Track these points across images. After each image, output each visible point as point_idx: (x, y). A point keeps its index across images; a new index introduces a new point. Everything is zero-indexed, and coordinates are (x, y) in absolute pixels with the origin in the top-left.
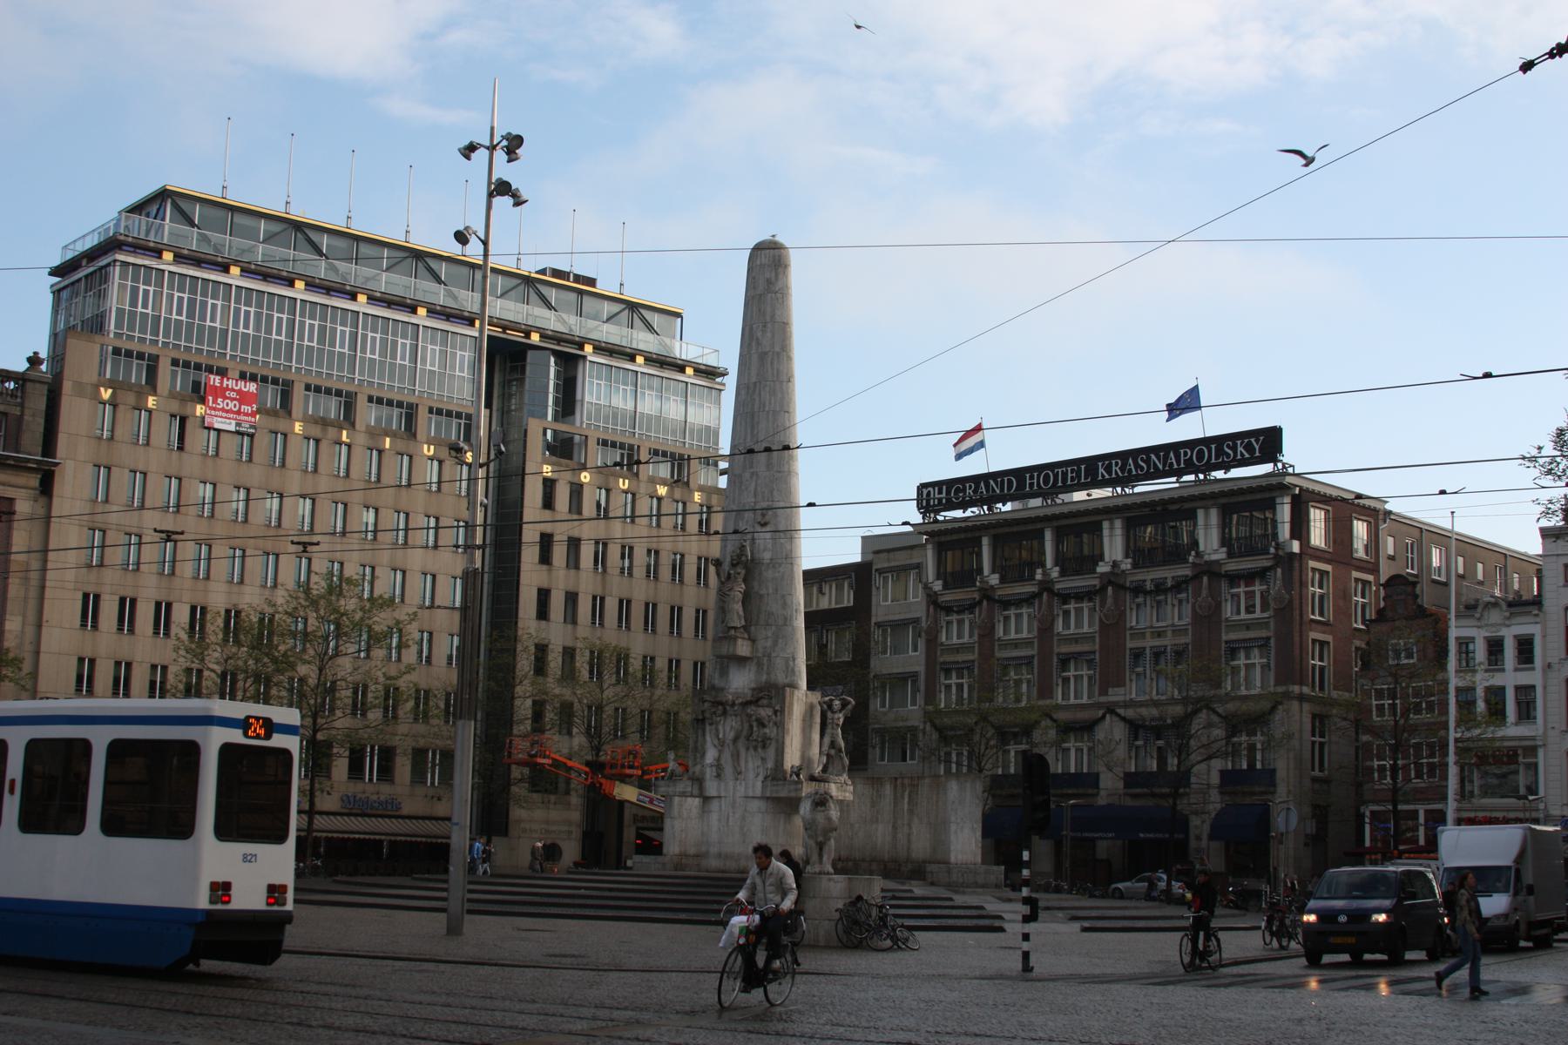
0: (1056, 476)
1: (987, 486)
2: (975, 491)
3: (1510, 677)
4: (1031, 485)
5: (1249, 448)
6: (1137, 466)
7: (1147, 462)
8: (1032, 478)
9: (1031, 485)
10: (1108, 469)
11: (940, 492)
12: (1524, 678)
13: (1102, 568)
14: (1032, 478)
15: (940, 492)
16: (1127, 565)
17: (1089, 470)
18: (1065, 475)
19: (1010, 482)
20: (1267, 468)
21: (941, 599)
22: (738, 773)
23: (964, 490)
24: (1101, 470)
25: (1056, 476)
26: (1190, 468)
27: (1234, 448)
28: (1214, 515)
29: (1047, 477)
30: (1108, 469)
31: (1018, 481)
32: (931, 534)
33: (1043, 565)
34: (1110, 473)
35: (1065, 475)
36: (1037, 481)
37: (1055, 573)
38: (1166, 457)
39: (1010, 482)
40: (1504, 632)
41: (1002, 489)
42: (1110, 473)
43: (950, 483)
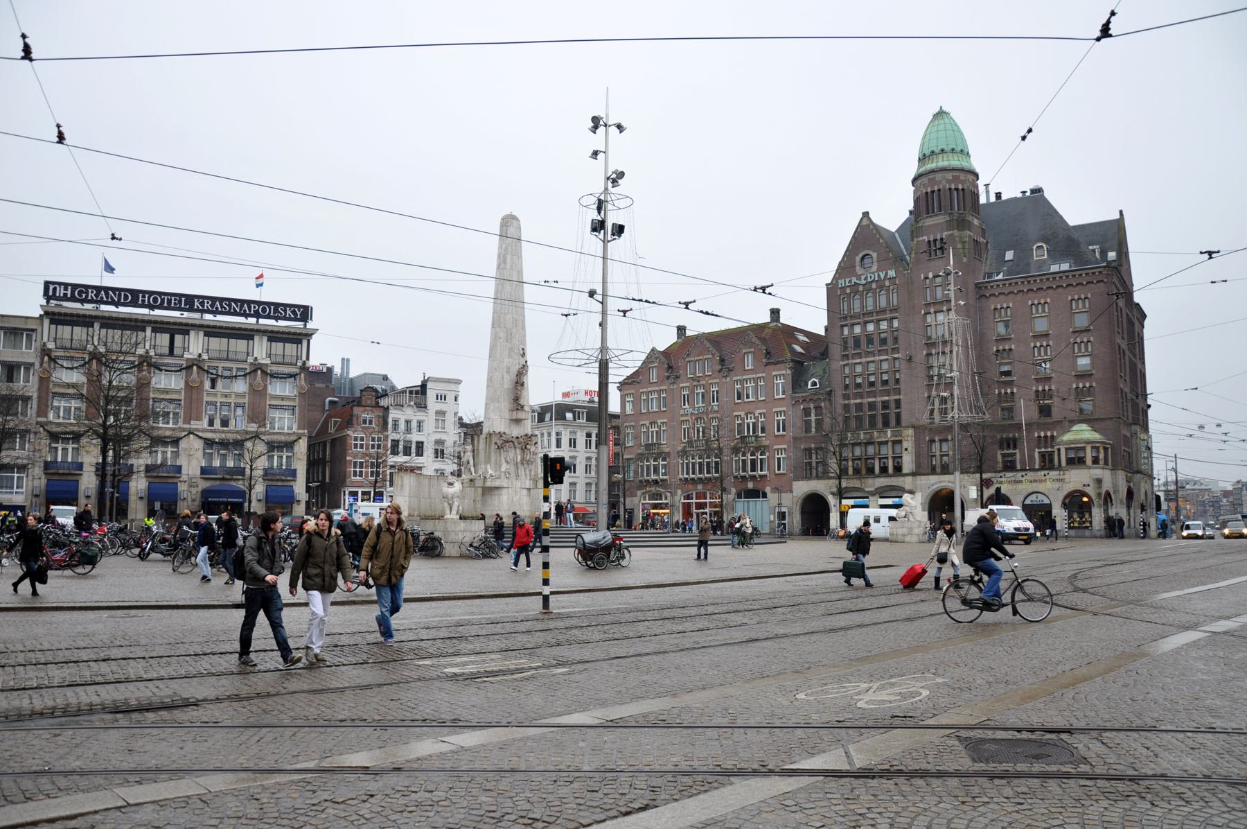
0: (163, 300)
2: (97, 296)
5: (294, 312)
7: (230, 306)
10: (202, 304)
11: (66, 289)
15: (66, 289)
17: (188, 301)
18: (169, 301)
20: (299, 324)
21: (53, 354)
22: (517, 475)
23: (87, 293)
25: (163, 300)
26: (257, 315)
27: (285, 311)
28: (265, 339)
30: (202, 304)
35: (169, 301)
43: (75, 286)
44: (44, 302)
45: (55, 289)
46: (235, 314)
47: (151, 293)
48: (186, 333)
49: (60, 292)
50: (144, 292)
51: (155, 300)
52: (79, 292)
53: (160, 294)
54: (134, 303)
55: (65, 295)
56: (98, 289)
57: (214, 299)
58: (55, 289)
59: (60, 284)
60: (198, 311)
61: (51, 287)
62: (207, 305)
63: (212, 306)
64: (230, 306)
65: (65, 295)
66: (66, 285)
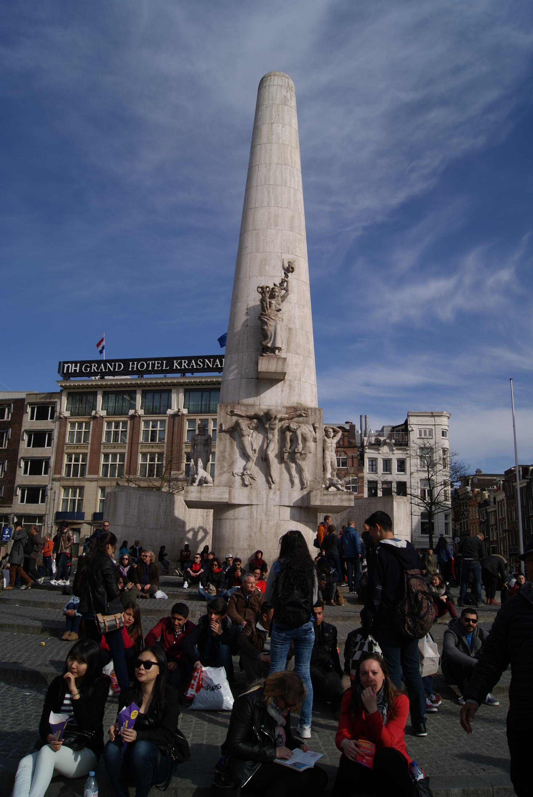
0: (148, 365)
1: (105, 366)
2: (97, 369)
3: (395, 476)
4: (133, 368)
6: (197, 364)
7: (204, 363)
8: (133, 364)
9: (133, 368)
10: (180, 364)
11: (76, 366)
12: (403, 478)
13: (170, 412)
14: (133, 364)
15: (76, 366)
16: (185, 411)
18: (153, 365)
19: (120, 366)
24: (175, 364)
25: (148, 365)
29: (143, 364)
30: (180, 364)
31: (125, 366)
32: (65, 388)
33: (133, 407)
34: (181, 366)
35: (153, 365)
36: (136, 366)
37: (141, 412)
38: (214, 362)
39: (120, 366)
40: (391, 456)
41: (115, 368)
42: (181, 366)
43: (82, 363)
44: (61, 378)
45: (68, 367)
46: (209, 370)
47: (138, 360)
48: (169, 392)
49: (72, 369)
50: (133, 360)
51: (142, 365)
52: (86, 368)
53: (146, 360)
54: (125, 372)
55: (75, 370)
56: (99, 362)
57: (190, 359)
58: (68, 367)
59: (72, 363)
60: (177, 371)
61: (66, 365)
62: (185, 364)
63: (188, 365)
64: (204, 363)
65: (75, 370)
66: (76, 363)
